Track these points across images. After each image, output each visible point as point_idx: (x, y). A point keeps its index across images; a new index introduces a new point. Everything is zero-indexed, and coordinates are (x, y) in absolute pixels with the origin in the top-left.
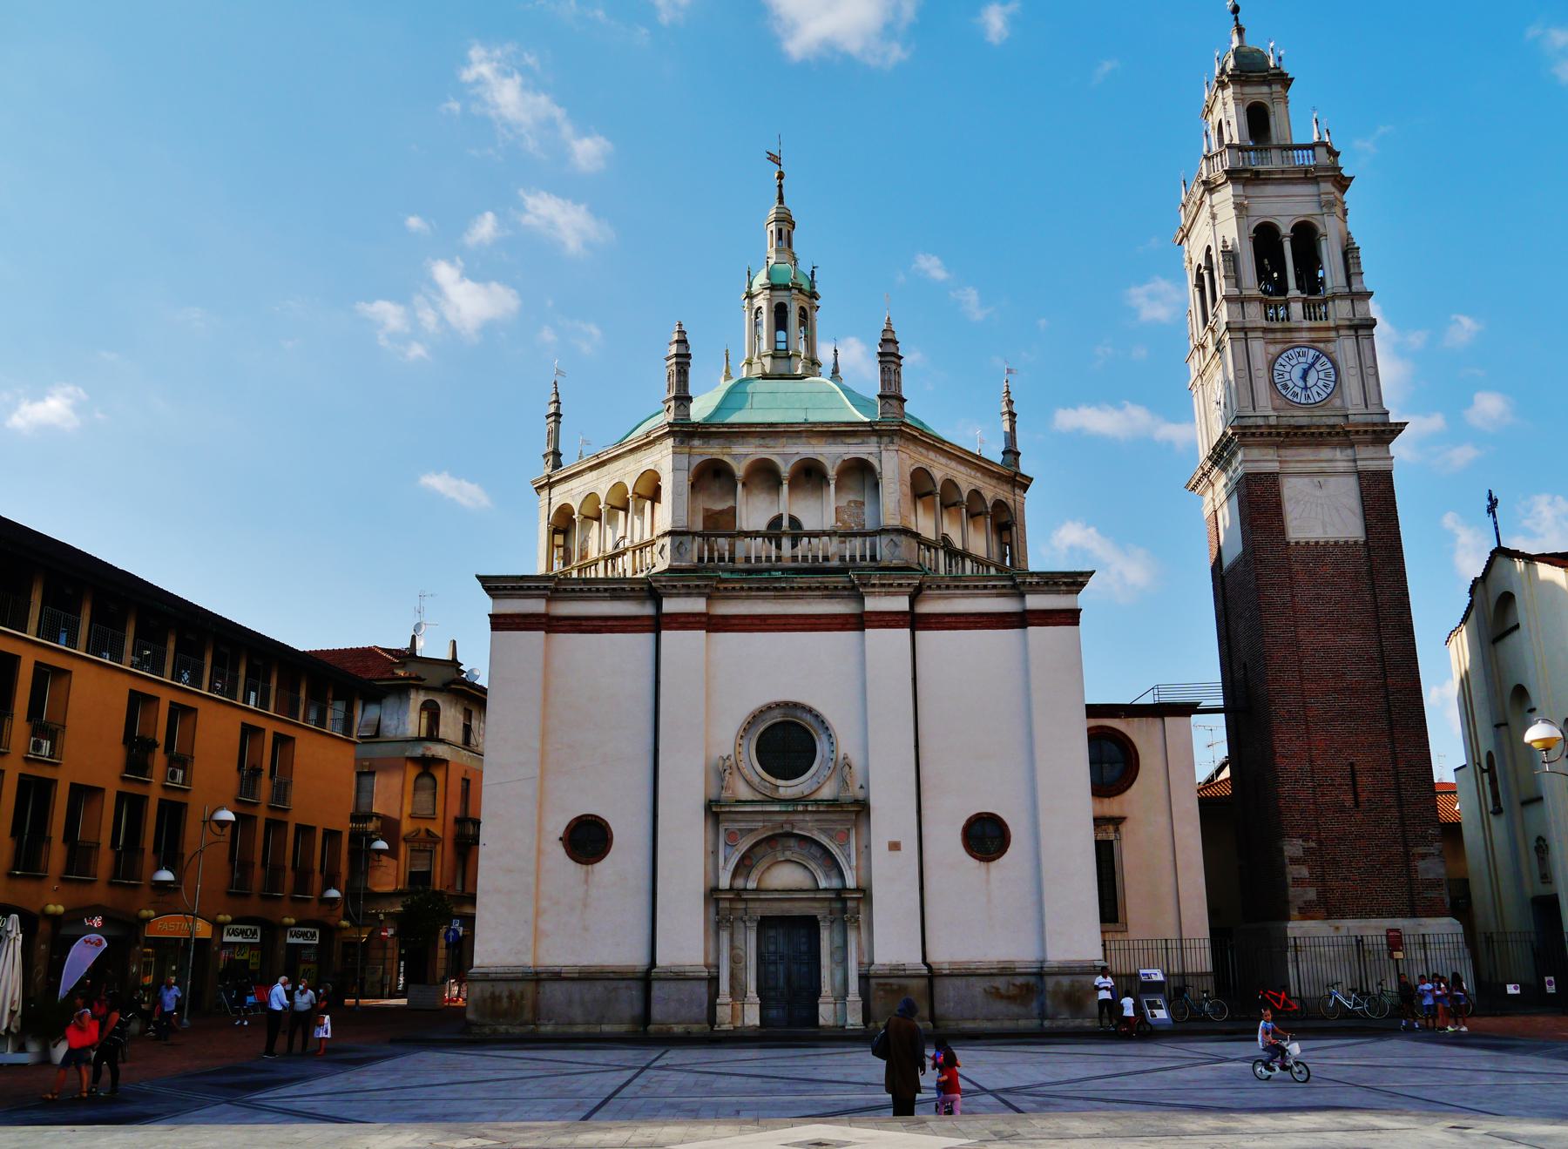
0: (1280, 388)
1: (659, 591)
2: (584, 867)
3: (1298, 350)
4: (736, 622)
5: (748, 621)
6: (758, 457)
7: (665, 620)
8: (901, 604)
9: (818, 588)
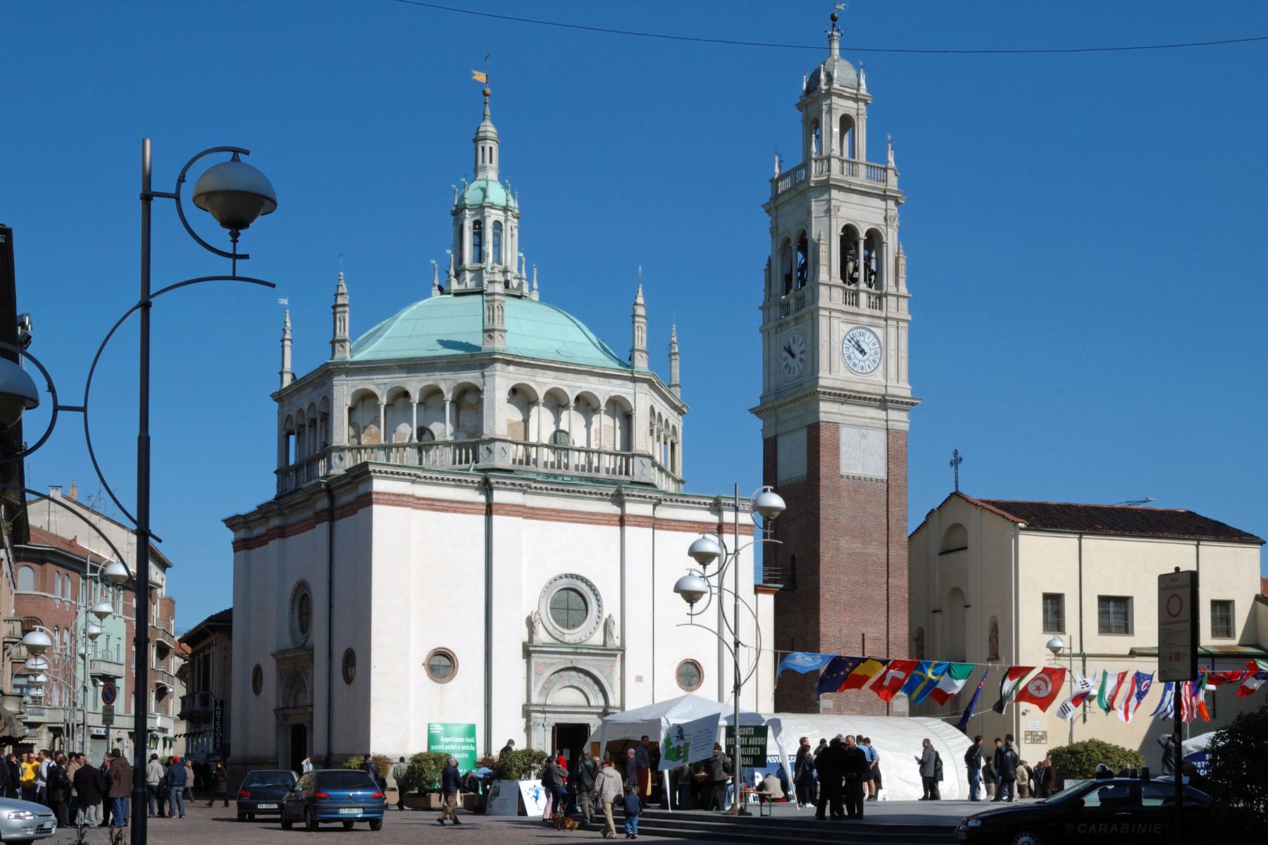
0: (846, 358)
1: (493, 486)
2: (439, 685)
3: (859, 330)
4: (540, 512)
5: (548, 513)
6: (553, 386)
7: (494, 507)
8: (645, 510)
9: (596, 493)
